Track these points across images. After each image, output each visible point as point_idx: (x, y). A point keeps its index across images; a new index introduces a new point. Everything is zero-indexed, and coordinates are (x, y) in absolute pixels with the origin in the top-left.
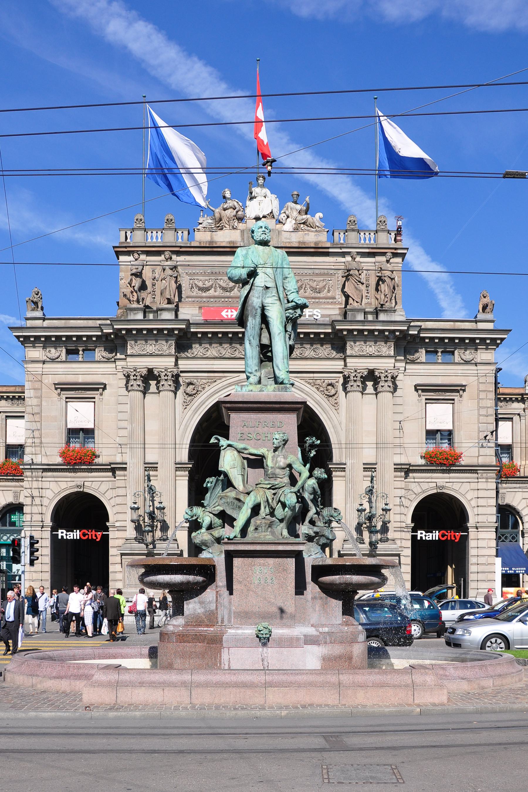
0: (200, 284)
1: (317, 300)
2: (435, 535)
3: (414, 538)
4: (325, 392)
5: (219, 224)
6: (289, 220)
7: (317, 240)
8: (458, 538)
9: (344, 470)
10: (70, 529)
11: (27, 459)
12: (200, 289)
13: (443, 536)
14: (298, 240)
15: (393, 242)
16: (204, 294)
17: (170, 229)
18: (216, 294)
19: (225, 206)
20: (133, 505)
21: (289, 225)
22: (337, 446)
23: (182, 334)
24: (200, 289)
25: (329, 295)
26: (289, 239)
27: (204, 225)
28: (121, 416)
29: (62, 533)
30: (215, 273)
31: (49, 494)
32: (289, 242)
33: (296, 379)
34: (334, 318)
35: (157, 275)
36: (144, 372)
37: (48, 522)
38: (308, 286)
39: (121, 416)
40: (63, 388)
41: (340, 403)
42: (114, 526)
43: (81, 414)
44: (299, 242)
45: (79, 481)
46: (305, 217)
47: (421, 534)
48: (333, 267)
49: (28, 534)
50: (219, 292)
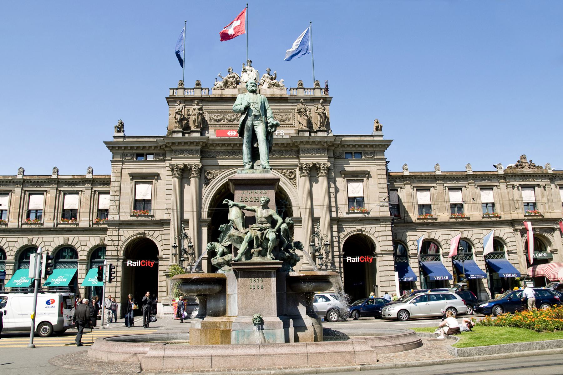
0: (215, 118)
2: (357, 259)
3: (345, 261)
5: (226, 85)
8: (371, 261)
10: (134, 260)
11: (110, 218)
12: (215, 120)
13: (362, 260)
16: (217, 123)
17: (198, 88)
18: (225, 123)
19: (229, 76)
20: (174, 245)
21: (265, 86)
22: (296, 208)
23: (204, 145)
24: (215, 120)
25: (289, 123)
27: (217, 86)
28: (169, 192)
29: (129, 263)
30: (224, 112)
31: (123, 239)
34: (292, 135)
35: (190, 113)
36: (182, 166)
37: (121, 255)
39: (169, 192)
40: (133, 177)
41: (297, 183)
42: (162, 258)
43: (144, 191)
45: (141, 231)
46: (274, 81)
47: (349, 259)
49: (109, 263)
50: (226, 122)
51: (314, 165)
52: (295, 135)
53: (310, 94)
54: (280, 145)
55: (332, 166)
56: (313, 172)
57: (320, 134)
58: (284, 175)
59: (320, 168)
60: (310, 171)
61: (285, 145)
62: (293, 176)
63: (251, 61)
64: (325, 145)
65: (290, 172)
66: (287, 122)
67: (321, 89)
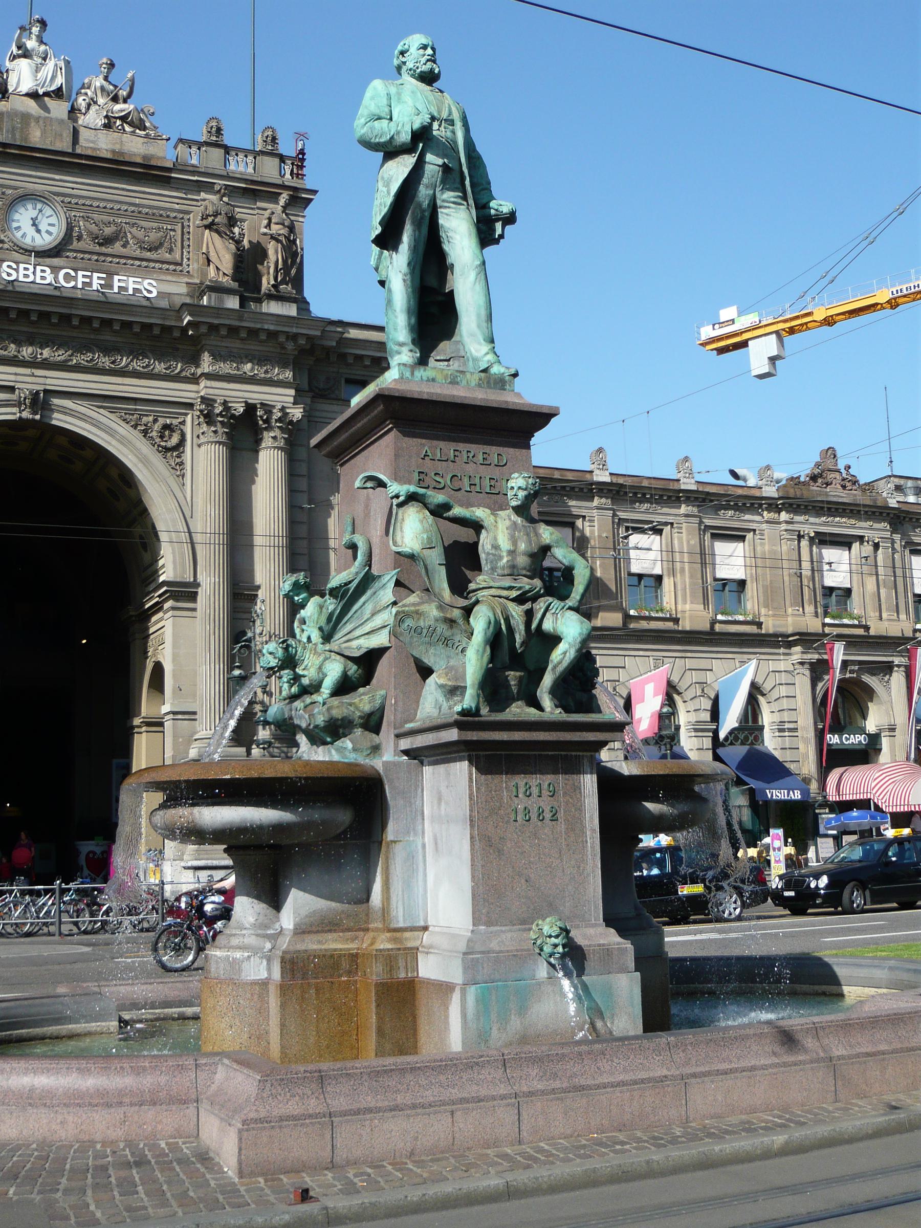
1: (145, 264)
4: (158, 440)
6: (94, 108)
7: (147, 152)
9: (193, 597)
14: (110, 147)
15: (288, 176)
26: (92, 142)
32: (94, 149)
33: (102, 411)
38: (129, 236)
44: (113, 152)
48: (177, 207)
51: (251, 408)
52: (188, 300)
53: (240, 166)
54: (137, 329)
55: (305, 420)
56: (242, 433)
57: (274, 308)
58: (145, 433)
59: (267, 421)
60: (232, 427)
61: (156, 331)
62: (175, 440)
63: (43, 23)
64: (290, 346)
65: (166, 427)
66: (163, 254)
67: (282, 159)
